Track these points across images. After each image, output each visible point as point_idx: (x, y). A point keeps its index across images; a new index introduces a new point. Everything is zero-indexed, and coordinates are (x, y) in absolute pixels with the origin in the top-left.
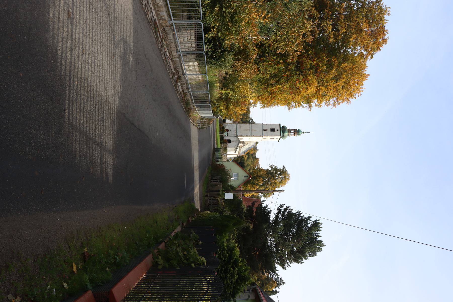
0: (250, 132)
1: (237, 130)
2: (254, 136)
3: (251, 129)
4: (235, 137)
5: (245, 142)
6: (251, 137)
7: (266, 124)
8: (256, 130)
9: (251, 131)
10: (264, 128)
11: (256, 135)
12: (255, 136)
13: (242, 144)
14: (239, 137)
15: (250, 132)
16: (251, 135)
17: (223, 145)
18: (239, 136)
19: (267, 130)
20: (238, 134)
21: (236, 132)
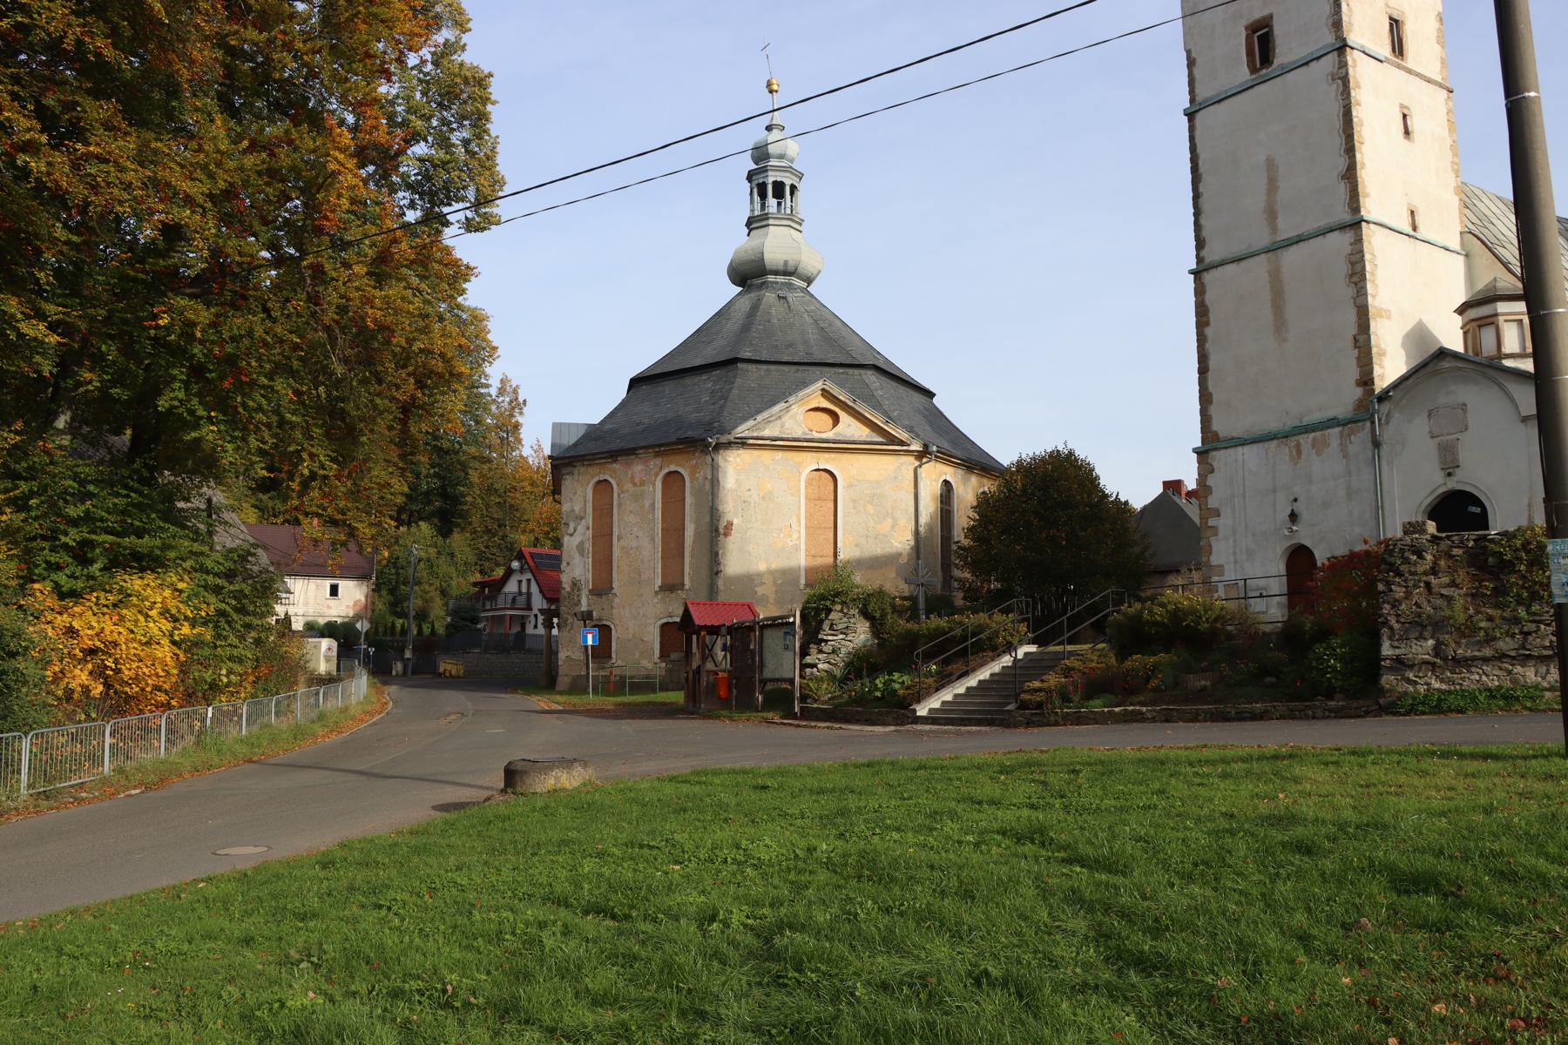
0: (1300, 240)
1: (1292, 423)
2: (1350, 175)
3: (1264, 240)
4: (1387, 434)
5: (1481, 285)
6: (1371, 208)
7: (1191, 63)
8: (1271, 165)
9: (1286, 230)
10: (1243, 74)
11: (1338, 141)
12: (1350, 150)
13: (1490, 321)
14: (1390, 367)
15: (1300, 240)
16: (1347, 217)
17: (1419, 626)
18: (1366, 380)
19: (1253, 28)
20: (1345, 399)
21: (1306, 440)
